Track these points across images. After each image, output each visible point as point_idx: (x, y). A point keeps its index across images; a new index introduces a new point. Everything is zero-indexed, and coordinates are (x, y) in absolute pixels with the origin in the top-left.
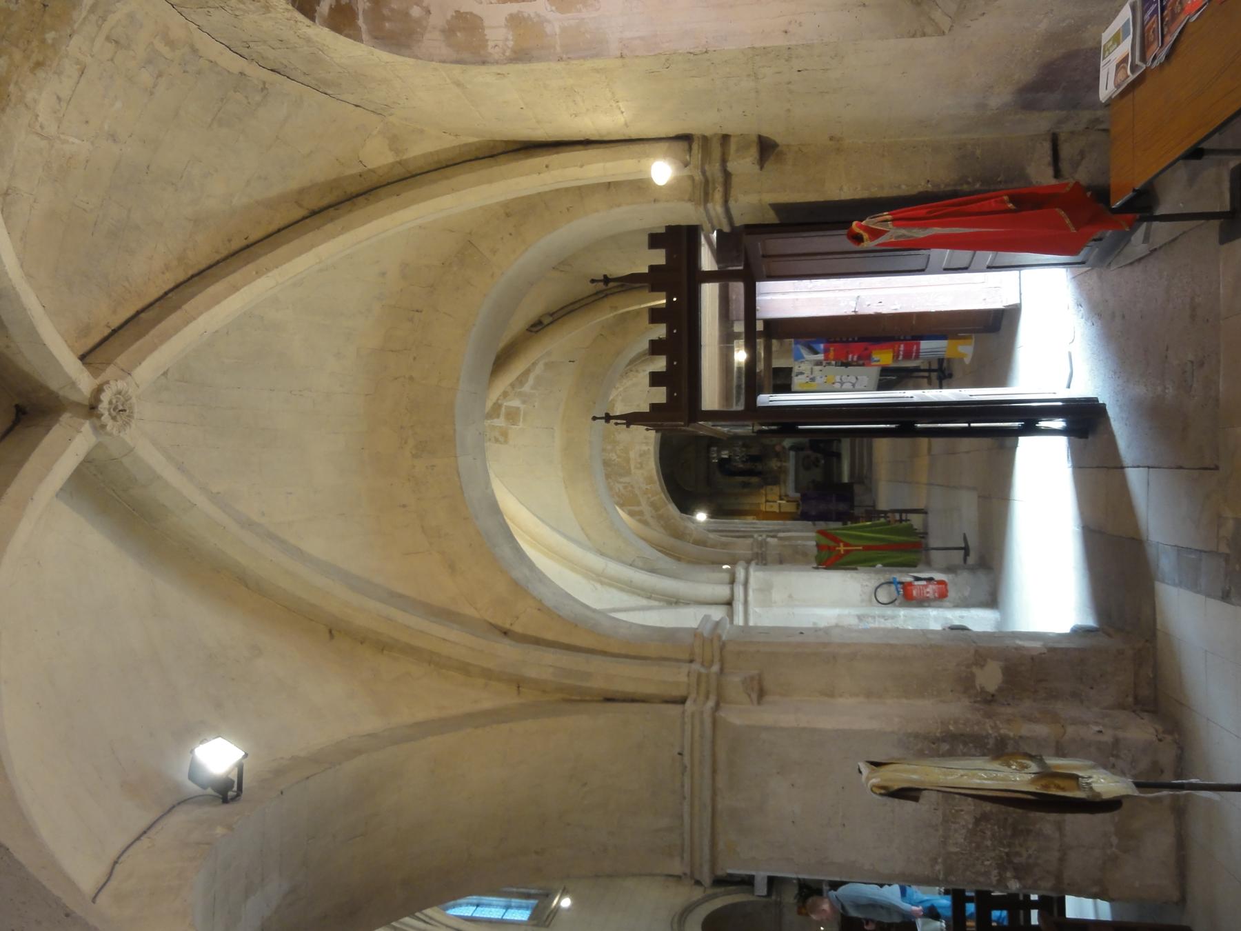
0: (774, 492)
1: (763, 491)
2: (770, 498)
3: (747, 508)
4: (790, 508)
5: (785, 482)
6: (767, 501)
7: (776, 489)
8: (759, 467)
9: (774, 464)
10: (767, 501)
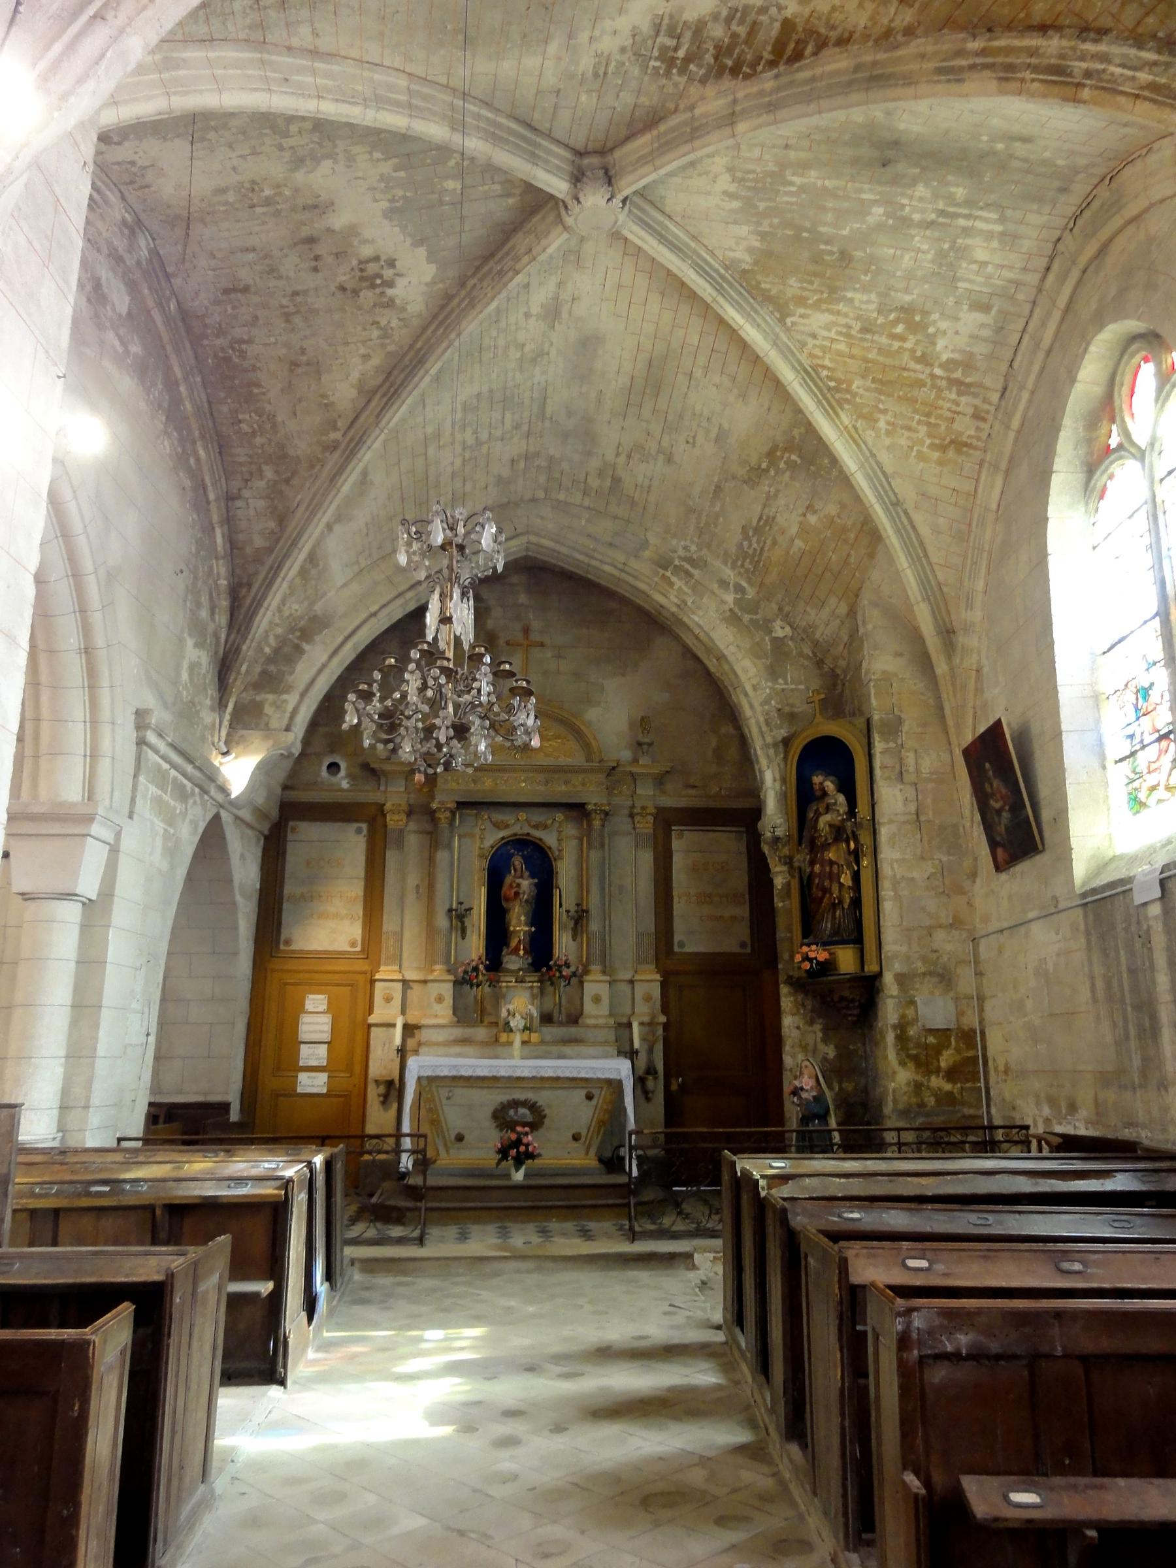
0: (436, 1007)
1: (439, 971)
2: (416, 992)
3: (389, 924)
4: (381, 1063)
5: (464, 1041)
6: (405, 983)
7: (443, 1013)
8: (514, 962)
9: (520, 1004)
10: (405, 983)
